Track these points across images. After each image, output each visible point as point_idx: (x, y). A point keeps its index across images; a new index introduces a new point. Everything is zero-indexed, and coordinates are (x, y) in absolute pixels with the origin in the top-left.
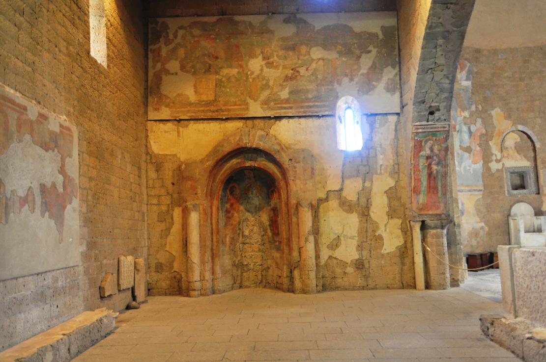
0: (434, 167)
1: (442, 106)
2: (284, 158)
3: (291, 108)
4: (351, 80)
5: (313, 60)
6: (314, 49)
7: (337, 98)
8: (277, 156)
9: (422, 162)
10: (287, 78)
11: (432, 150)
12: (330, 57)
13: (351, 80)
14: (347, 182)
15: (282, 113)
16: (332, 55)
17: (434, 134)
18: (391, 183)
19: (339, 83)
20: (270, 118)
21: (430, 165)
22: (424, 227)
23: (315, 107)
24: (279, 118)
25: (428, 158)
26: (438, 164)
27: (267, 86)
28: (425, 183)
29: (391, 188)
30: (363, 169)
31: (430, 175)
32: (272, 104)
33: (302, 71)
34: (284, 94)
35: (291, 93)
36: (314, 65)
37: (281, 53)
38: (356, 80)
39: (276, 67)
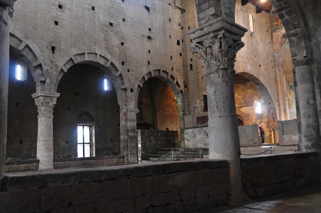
0: (274, 116)
1: (271, 102)
2: (242, 116)
3: (244, 104)
4: (257, 96)
5: (248, 93)
6: (248, 90)
7: (254, 101)
8: (241, 116)
9: (271, 115)
10: (243, 98)
11: (272, 111)
12: (252, 91)
13: (257, 96)
14: (257, 120)
15: (242, 106)
16: (252, 91)
17: (272, 108)
18: (267, 120)
19: (254, 97)
20: (239, 107)
21: (273, 115)
22: (274, 130)
23: (249, 103)
24: (242, 107)
25: (272, 114)
26: (274, 115)
27: (239, 100)
28: (272, 120)
29: (267, 121)
30: (261, 117)
31: (273, 117)
32: (240, 104)
33: (246, 95)
34: (242, 101)
35: (244, 101)
36: (248, 94)
37: (241, 92)
38: (258, 96)
39: (241, 95)
